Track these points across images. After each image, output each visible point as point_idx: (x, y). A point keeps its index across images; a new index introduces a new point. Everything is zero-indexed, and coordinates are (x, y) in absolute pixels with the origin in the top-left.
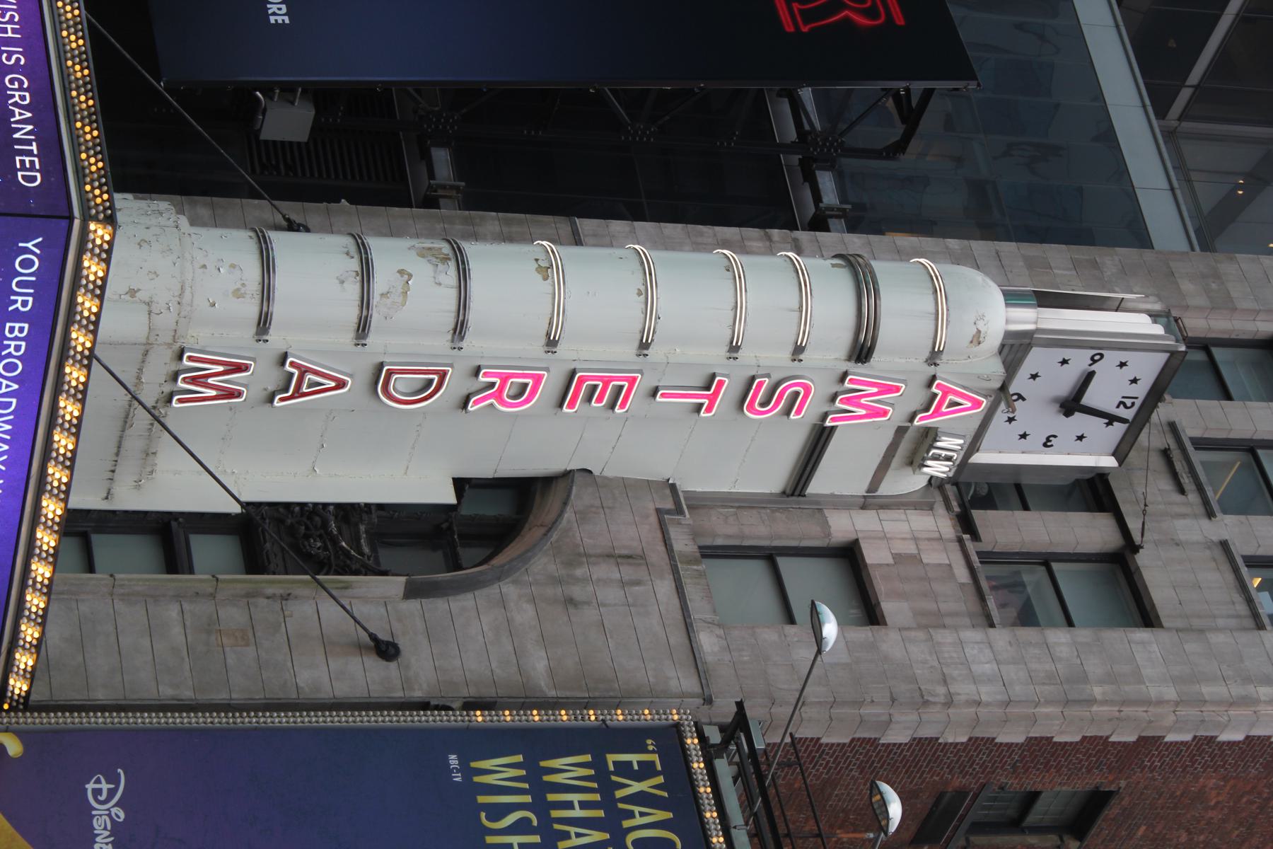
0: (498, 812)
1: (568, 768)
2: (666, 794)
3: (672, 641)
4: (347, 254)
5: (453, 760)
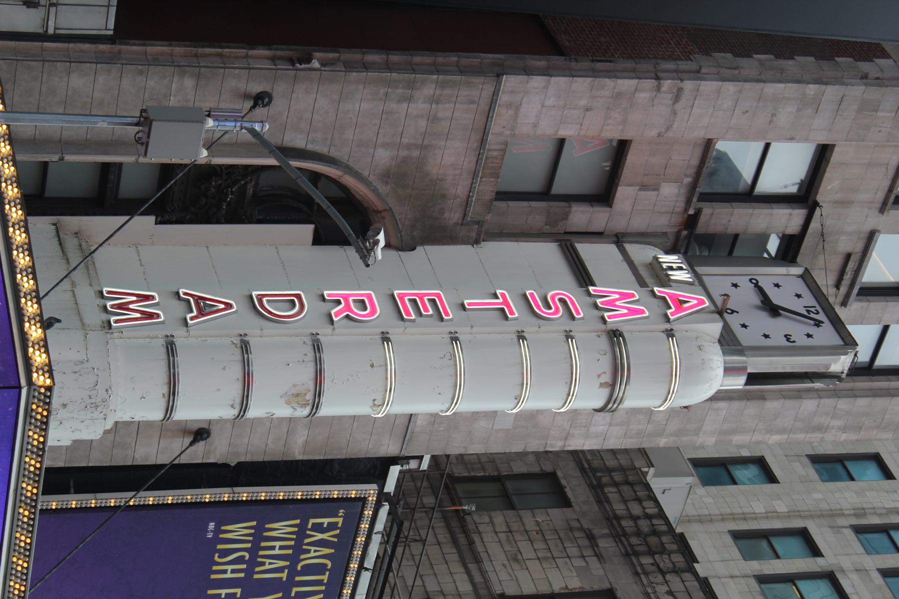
0: (225, 553)
1: (282, 528)
2: (336, 540)
3: (397, 422)
4: (232, 406)
5: (212, 526)
